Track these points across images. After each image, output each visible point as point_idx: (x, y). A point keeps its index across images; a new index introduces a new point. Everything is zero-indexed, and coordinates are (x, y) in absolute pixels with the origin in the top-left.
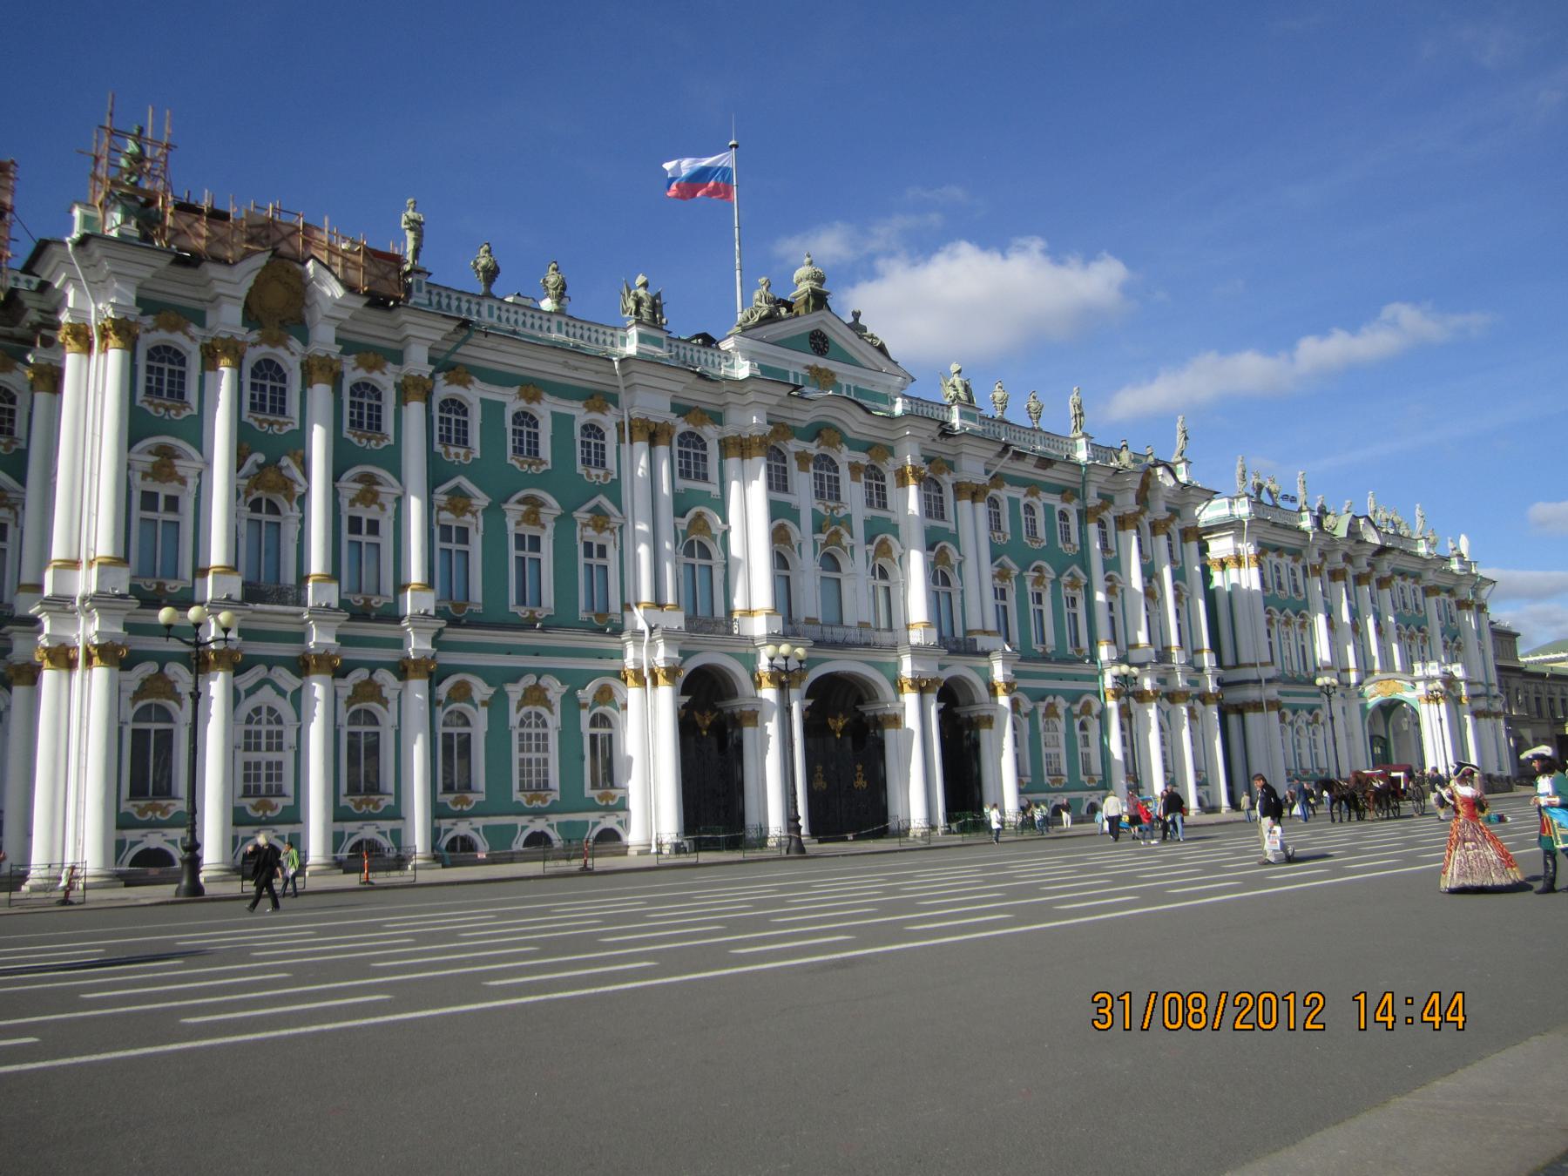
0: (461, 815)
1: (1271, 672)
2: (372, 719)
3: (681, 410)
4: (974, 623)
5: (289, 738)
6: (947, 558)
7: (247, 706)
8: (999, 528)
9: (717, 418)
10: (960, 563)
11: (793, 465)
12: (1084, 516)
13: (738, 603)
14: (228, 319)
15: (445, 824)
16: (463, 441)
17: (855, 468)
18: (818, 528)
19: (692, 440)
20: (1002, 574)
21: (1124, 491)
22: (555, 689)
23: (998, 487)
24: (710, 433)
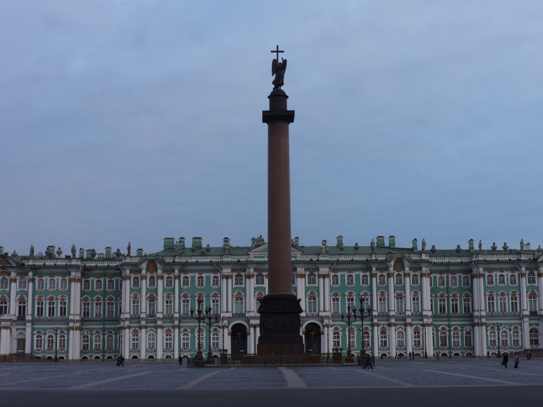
0: (185, 352)
1: (483, 313)
2: (170, 335)
4: (322, 309)
5: (155, 339)
6: (314, 293)
7: (148, 334)
8: (337, 283)
9: (244, 270)
10: (319, 294)
11: (265, 278)
12: (372, 276)
13: (247, 310)
15: (182, 353)
16: (188, 285)
20: (336, 295)
21: (389, 267)
23: (337, 272)
24: (242, 274)
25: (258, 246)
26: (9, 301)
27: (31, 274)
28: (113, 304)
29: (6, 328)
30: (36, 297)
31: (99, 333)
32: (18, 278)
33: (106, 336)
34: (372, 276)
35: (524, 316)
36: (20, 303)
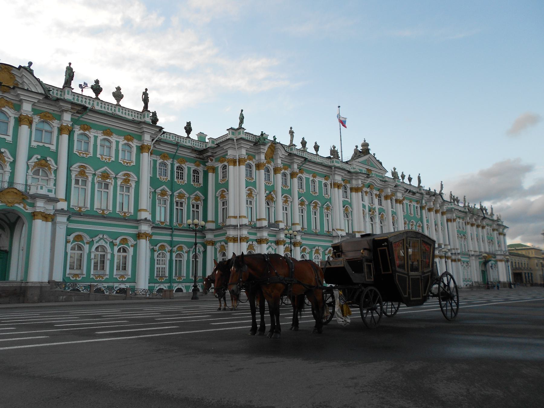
1: (459, 251)
3: (344, 180)
12: (422, 208)
14: (263, 157)
17: (376, 195)
18: (370, 211)
19: (345, 188)
20: (405, 223)
22: (321, 250)
24: (348, 186)
25: (360, 156)
26: (13, 164)
27: (67, 117)
28: (181, 204)
29: (46, 217)
30: (75, 167)
31: (165, 250)
32: (36, 119)
33: (174, 255)
34: (422, 208)
35: (473, 255)
36: (36, 173)
